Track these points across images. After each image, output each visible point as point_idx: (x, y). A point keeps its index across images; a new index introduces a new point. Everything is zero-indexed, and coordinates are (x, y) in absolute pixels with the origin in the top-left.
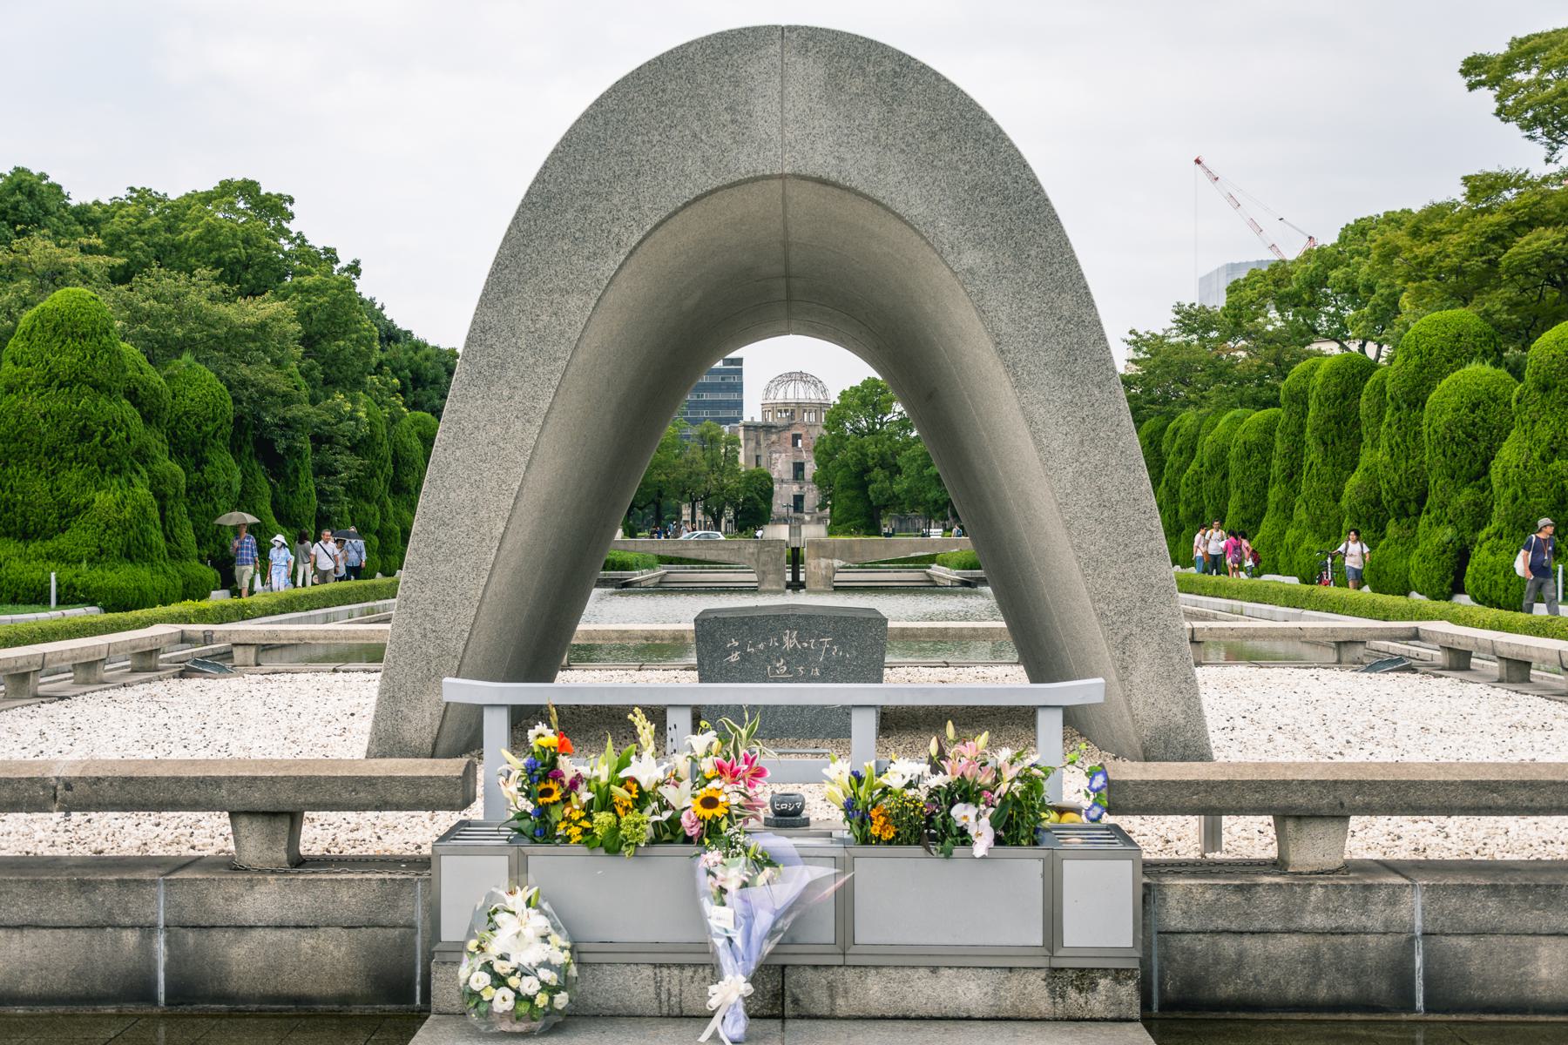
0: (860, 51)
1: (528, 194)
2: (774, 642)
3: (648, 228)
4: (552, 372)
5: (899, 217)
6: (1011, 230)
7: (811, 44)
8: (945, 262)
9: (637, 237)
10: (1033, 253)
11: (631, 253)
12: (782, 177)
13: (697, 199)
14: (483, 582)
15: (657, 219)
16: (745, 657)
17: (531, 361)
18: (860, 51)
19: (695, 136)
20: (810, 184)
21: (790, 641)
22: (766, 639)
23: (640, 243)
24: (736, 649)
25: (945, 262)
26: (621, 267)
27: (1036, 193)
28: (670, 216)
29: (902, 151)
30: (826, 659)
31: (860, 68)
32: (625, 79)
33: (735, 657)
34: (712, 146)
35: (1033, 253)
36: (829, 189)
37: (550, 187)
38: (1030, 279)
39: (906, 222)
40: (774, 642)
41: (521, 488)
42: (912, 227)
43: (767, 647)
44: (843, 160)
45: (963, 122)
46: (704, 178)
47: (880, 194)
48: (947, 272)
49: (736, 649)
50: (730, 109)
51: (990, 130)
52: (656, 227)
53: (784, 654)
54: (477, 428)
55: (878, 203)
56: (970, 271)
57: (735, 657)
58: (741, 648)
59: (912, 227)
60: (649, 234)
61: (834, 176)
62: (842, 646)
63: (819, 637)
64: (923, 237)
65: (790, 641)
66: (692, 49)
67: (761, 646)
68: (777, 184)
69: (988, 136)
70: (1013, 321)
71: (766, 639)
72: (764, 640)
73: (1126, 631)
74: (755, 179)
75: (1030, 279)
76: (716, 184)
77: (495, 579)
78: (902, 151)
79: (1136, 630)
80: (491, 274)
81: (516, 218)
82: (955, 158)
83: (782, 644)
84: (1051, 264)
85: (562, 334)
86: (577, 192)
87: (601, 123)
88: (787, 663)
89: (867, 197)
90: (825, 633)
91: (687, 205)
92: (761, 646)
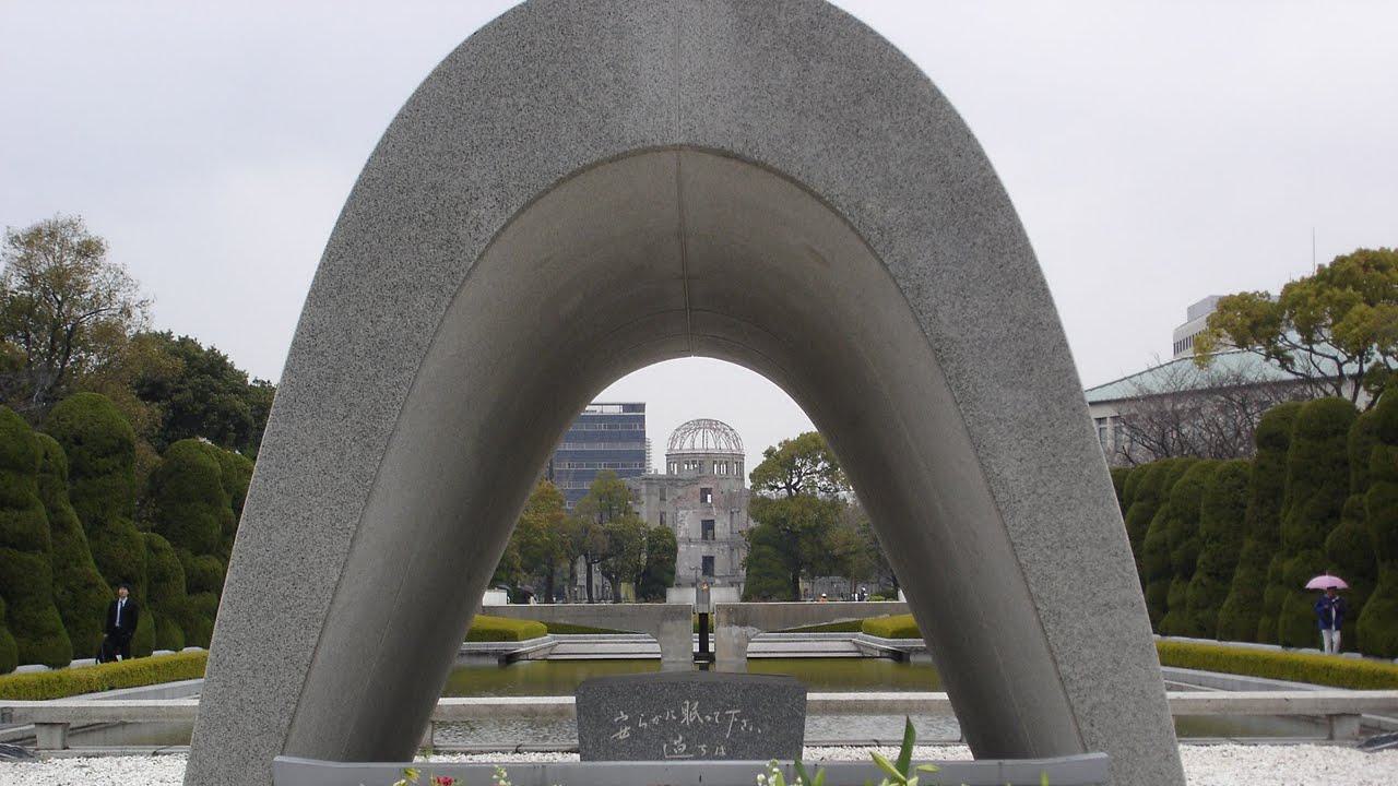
1: (367, 168)
2: (670, 715)
3: (514, 209)
5: (819, 198)
8: (873, 251)
9: (501, 220)
10: (979, 241)
11: (493, 240)
12: (679, 148)
13: (573, 175)
14: (313, 642)
15: (523, 200)
16: (636, 734)
17: (371, 371)
20: (710, 158)
21: (690, 714)
22: (662, 712)
23: (504, 228)
24: (624, 724)
25: (873, 251)
26: (481, 256)
28: (539, 197)
31: (769, 17)
32: (485, 29)
33: (624, 734)
34: (590, 111)
35: (979, 241)
36: (733, 163)
37: (393, 160)
38: (976, 272)
39: (826, 204)
40: (670, 715)
42: (833, 209)
43: (662, 721)
44: (750, 127)
45: (894, 82)
47: (795, 170)
48: (876, 265)
49: (624, 724)
52: (522, 211)
53: (684, 729)
54: (305, 453)
55: (792, 180)
57: (624, 734)
59: (833, 209)
60: (516, 216)
61: (738, 147)
62: (753, 720)
63: (725, 708)
64: (845, 220)
65: (690, 714)
67: (655, 720)
69: (924, 99)
70: (956, 323)
71: (662, 712)
73: (1095, 699)
74: (645, 151)
75: (976, 272)
76: (595, 157)
79: (1107, 698)
84: (1001, 255)
89: (778, 173)
90: (733, 705)
91: (560, 182)
92: (655, 720)
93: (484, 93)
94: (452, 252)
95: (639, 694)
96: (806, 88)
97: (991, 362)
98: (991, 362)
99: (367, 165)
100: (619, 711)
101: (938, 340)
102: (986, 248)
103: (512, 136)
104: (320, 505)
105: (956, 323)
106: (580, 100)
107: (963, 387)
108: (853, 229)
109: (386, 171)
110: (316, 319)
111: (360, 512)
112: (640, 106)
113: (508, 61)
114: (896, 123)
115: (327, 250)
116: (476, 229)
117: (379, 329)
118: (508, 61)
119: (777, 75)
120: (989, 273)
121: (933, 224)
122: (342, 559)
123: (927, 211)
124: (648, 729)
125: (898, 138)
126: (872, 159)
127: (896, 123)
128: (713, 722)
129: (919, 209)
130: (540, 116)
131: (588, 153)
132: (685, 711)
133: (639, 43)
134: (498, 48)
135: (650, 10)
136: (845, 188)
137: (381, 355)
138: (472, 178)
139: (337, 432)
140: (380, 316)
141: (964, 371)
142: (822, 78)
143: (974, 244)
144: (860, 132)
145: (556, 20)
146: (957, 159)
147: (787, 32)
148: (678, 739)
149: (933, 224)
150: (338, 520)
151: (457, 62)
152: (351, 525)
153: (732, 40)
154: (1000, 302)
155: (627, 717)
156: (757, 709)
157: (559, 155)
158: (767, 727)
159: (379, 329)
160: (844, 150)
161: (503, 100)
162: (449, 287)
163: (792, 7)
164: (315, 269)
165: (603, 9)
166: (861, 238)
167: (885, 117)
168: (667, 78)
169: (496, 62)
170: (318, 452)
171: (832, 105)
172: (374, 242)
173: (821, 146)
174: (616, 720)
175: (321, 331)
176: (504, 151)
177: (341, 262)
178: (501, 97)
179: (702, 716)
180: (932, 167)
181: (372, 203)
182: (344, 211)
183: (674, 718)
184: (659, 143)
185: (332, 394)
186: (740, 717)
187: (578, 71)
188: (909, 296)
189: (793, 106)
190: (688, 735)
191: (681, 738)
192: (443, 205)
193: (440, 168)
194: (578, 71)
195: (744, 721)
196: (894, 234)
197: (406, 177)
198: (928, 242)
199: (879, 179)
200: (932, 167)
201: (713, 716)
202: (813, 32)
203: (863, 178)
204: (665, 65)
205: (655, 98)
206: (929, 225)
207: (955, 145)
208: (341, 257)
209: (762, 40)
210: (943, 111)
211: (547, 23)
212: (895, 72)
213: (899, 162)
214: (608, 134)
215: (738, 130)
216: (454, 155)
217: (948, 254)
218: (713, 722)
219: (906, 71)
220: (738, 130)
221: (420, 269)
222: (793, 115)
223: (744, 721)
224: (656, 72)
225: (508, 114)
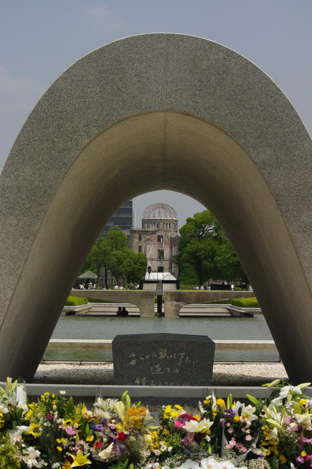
0: (207, 47)
1: (29, 118)
3: (93, 136)
4: (39, 212)
6: (285, 141)
7: (181, 43)
9: (87, 141)
10: (296, 153)
16: (139, 363)
17: (29, 205)
18: (207, 47)
19: (119, 89)
20: (179, 115)
23: (88, 144)
24: (134, 358)
26: (77, 157)
27: (298, 123)
29: (228, 99)
30: (182, 364)
31: (206, 56)
33: (133, 363)
37: (41, 114)
38: (295, 167)
40: (154, 355)
41: (21, 272)
43: (151, 357)
45: (260, 85)
46: (123, 111)
49: (134, 358)
50: (137, 75)
51: (274, 89)
56: (264, 162)
57: (133, 363)
65: (162, 356)
66: (118, 45)
67: (148, 357)
68: (161, 114)
75: (295, 167)
77: (6, 321)
78: (228, 99)
80: (9, 159)
81: (23, 130)
82: (256, 103)
84: (305, 160)
85: (45, 192)
86: (56, 118)
87: (69, 81)
88: (161, 366)
92: (148, 357)
93: (81, 86)
94: (65, 154)
95: (140, 345)
96: (222, 86)
97: (301, 206)
98: (301, 206)
99: (29, 117)
100: (131, 353)
101: (277, 196)
102: (299, 157)
103: (93, 105)
104: (5, 263)
105: (286, 189)
106: (123, 90)
107: (289, 216)
108: (241, 147)
109: (38, 119)
110: (5, 183)
111: (22, 266)
112: (149, 92)
113: (92, 73)
114: (261, 102)
115: (11, 153)
116: (76, 144)
117: (32, 187)
118: (92, 73)
119: (209, 80)
120: (300, 167)
121: (276, 145)
122: (14, 287)
123: (273, 140)
124: (144, 361)
125: (262, 108)
126: (250, 117)
127: (261, 102)
128: (173, 358)
129: (270, 139)
130: (105, 96)
131: (126, 112)
132: (161, 353)
133: (149, 66)
134: (88, 67)
135: (155, 52)
136: (238, 129)
137: (33, 198)
138: (75, 122)
139: (13, 231)
140: (33, 182)
141: (289, 209)
142: (229, 82)
143: (294, 155)
144: (245, 106)
145: (114, 56)
146: (287, 118)
147: (214, 62)
148: (157, 365)
149: (276, 145)
150: (13, 270)
151: (70, 73)
152: (18, 272)
153: (190, 65)
154: (305, 180)
155: (135, 355)
157: (113, 113)
158: (197, 361)
159: (32, 187)
160: (238, 113)
161: (89, 89)
162: (64, 169)
163: (216, 52)
164: (5, 161)
165: (134, 51)
166: (245, 151)
167: (256, 100)
168: (161, 81)
169: (87, 73)
170: (5, 240)
171: (233, 93)
172: (31, 150)
173: (228, 111)
174: (130, 356)
175: (7, 188)
176: (88, 111)
177: (17, 158)
178: (88, 88)
179: (168, 355)
180: (276, 121)
181: (31, 133)
182: (19, 136)
183: (156, 356)
184: (157, 109)
185: (11, 215)
187: (122, 77)
188: (266, 176)
189: (216, 94)
190: (162, 364)
191: (159, 365)
192: (62, 134)
193: (61, 118)
194: (122, 77)
195: (187, 358)
196: (259, 150)
197: (46, 122)
198: (274, 153)
199: (253, 125)
200: (276, 121)
201: (173, 355)
202: (225, 63)
203: (246, 126)
204: (161, 75)
205: (156, 90)
206: (275, 146)
207: (286, 112)
208: (17, 156)
209: (203, 66)
210: (281, 98)
211: (110, 57)
212: (261, 81)
213: (262, 119)
214: (135, 104)
215: (192, 104)
216: (67, 113)
217: (282, 159)
218: (173, 358)
219: (265, 80)
220: (192, 104)
221: (51, 161)
222: (216, 98)
223: (187, 358)
224: (156, 79)
225: (92, 96)
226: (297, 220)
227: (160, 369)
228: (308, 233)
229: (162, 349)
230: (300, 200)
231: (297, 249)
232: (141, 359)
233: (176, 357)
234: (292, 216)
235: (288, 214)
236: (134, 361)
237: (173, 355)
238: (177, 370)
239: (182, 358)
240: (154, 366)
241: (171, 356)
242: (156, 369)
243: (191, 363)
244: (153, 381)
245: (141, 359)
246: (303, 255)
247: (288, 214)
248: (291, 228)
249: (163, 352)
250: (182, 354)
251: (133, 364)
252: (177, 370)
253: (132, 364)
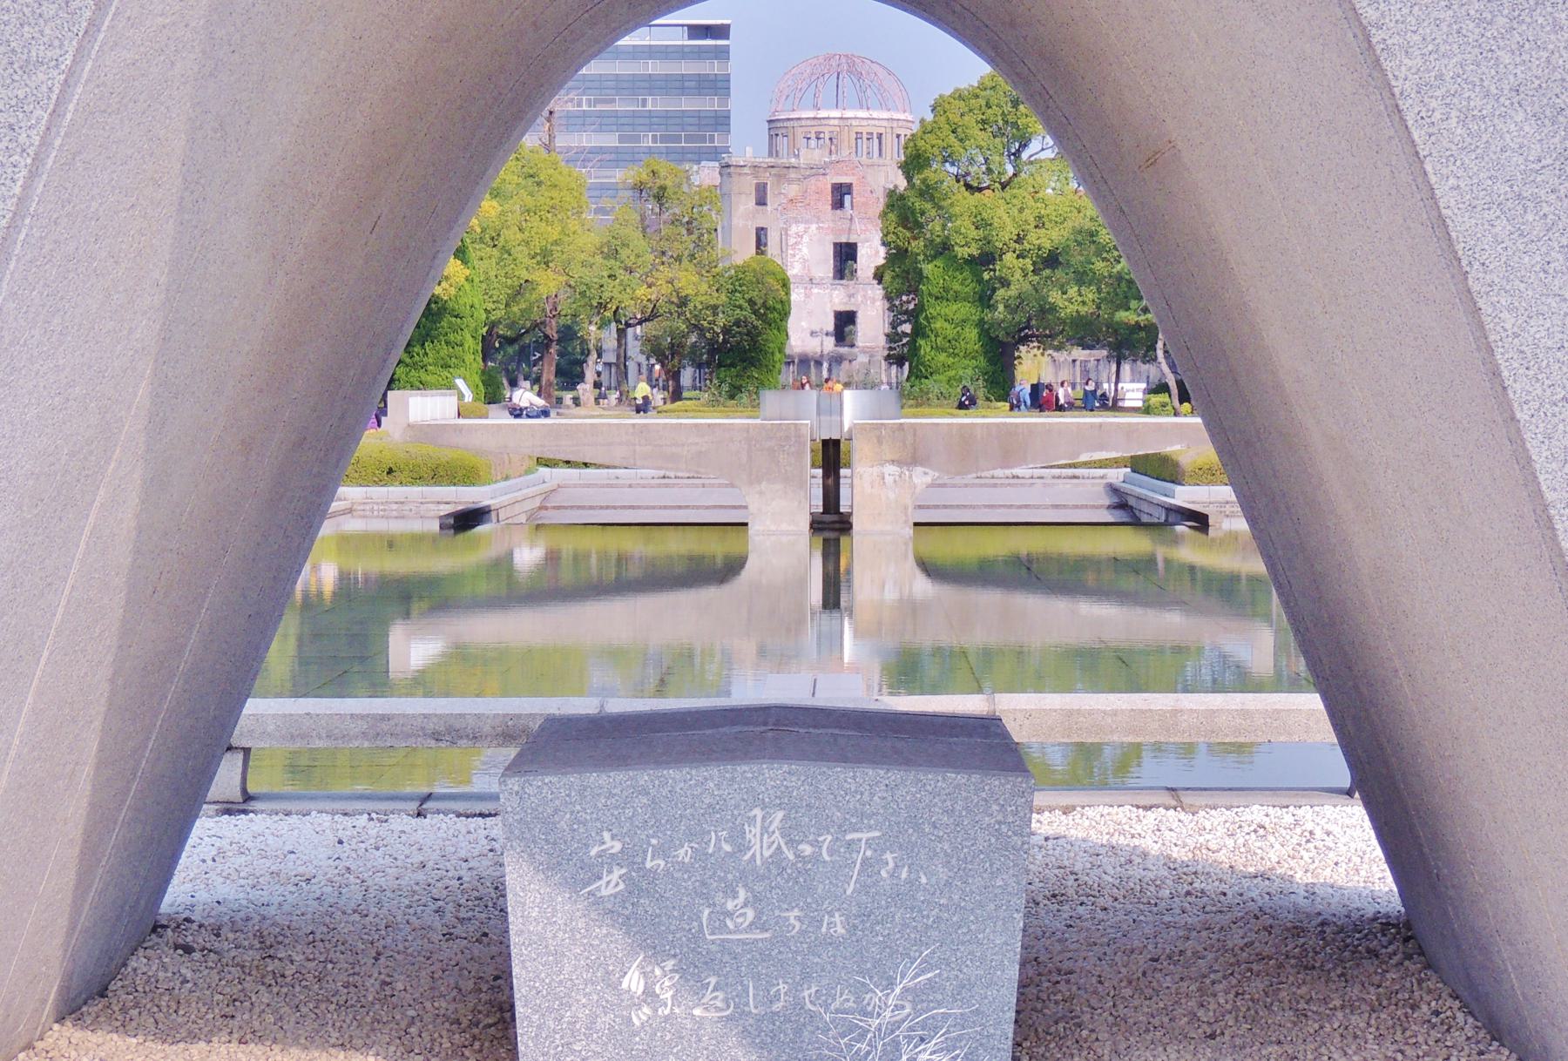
2: (718, 842)
30: (864, 888)
40: (718, 842)
58: (630, 858)
65: (762, 842)
67: (684, 853)
72: (690, 835)
83: (742, 848)
88: (755, 900)
92: (684, 853)
97: (1506, 58)
98: (1506, 58)
107: (1437, 115)
124: (667, 872)
128: (816, 858)
132: (753, 833)
141: (1440, 77)
155: (618, 846)
156: (917, 828)
158: (943, 873)
174: (593, 852)
179: (791, 843)
183: (727, 848)
186: (878, 847)
191: (742, 894)
195: (889, 856)
201: (816, 844)
218: (816, 858)
223: (889, 856)
226: (1485, 137)
227: (750, 914)
228: (1546, 209)
229: (757, 812)
230: (1501, 21)
231: (1481, 303)
232: (649, 865)
233: (831, 852)
234: (1454, 113)
235: (1434, 104)
236: (615, 876)
237: (816, 844)
238: (837, 918)
239: (865, 861)
240: (719, 898)
241: (807, 849)
242: (730, 914)
243: (909, 882)
244: (713, 980)
245: (649, 865)
246: (1516, 335)
247: (1434, 104)
248: (1452, 181)
249: (765, 830)
250: (864, 836)
251: (610, 891)
252: (837, 918)
253: (604, 892)
